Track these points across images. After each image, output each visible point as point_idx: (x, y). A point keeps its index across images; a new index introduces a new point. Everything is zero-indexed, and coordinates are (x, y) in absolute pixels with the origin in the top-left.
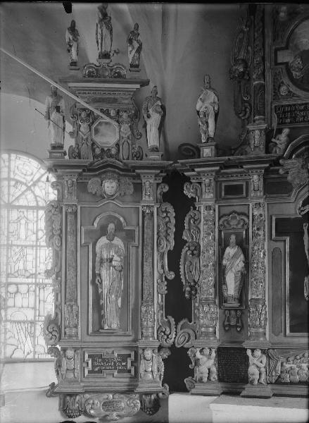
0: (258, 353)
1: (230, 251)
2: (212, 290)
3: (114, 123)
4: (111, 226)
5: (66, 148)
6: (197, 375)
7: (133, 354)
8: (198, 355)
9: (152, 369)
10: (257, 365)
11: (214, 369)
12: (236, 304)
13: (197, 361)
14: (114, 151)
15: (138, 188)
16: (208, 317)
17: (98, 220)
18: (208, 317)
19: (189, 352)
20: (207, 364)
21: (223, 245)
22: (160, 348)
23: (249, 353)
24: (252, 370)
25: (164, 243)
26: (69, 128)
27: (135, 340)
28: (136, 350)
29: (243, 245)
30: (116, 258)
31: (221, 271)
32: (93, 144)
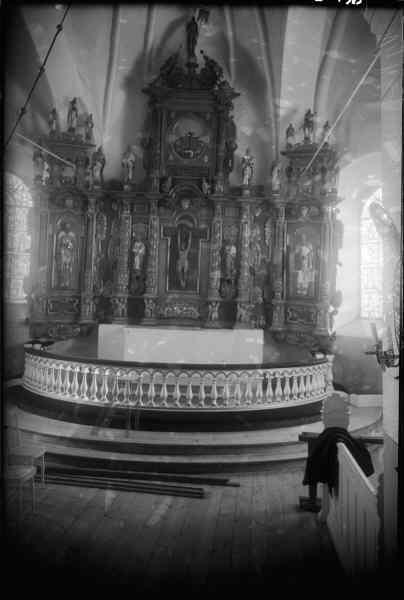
0: (151, 301)
1: (138, 244)
2: (126, 265)
3: (74, 166)
4: (68, 226)
5: (44, 179)
6: (115, 312)
7: (77, 301)
8: (117, 302)
9: (89, 309)
10: (149, 307)
11: (126, 310)
12: (139, 274)
13: (117, 306)
14: (73, 181)
15: (86, 203)
16: (123, 279)
17: (60, 221)
18: (123, 279)
19: (111, 301)
20: (122, 307)
21: (133, 240)
22: (95, 297)
23: (146, 301)
24: (147, 310)
25: (99, 236)
26: (47, 166)
27: (80, 293)
28: (79, 298)
29: (146, 241)
30: (70, 244)
31: (132, 255)
32: (61, 176)
